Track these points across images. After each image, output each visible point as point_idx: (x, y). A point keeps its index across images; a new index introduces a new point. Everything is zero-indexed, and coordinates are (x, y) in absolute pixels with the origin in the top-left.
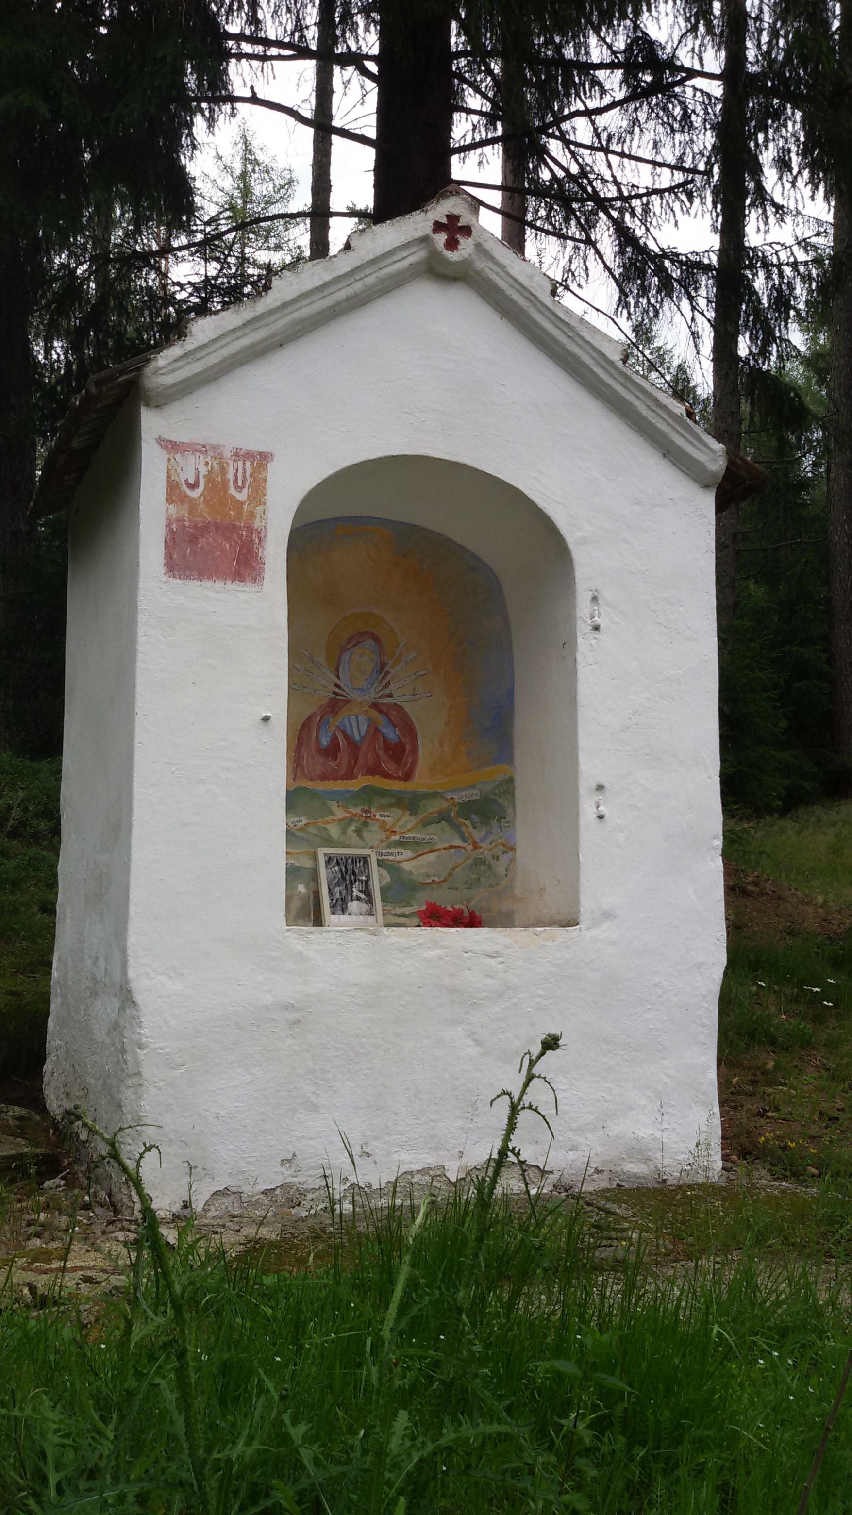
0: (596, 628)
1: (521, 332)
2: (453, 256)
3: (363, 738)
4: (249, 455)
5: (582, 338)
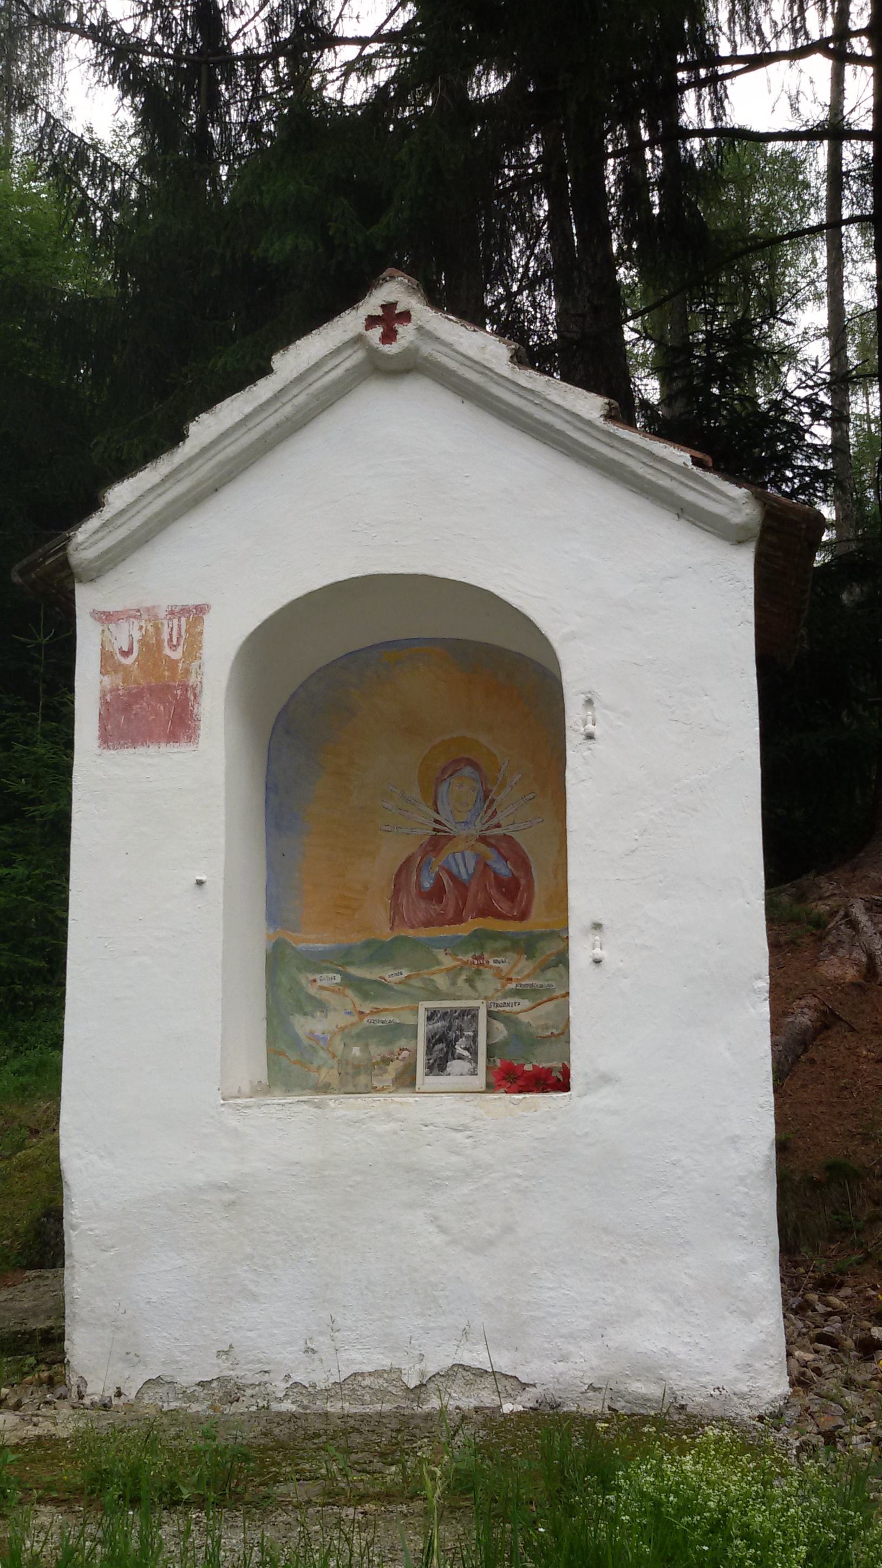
0: (590, 737)
1: (484, 409)
2: (391, 349)
3: (471, 876)
4: (185, 610)
5: (550, 402)
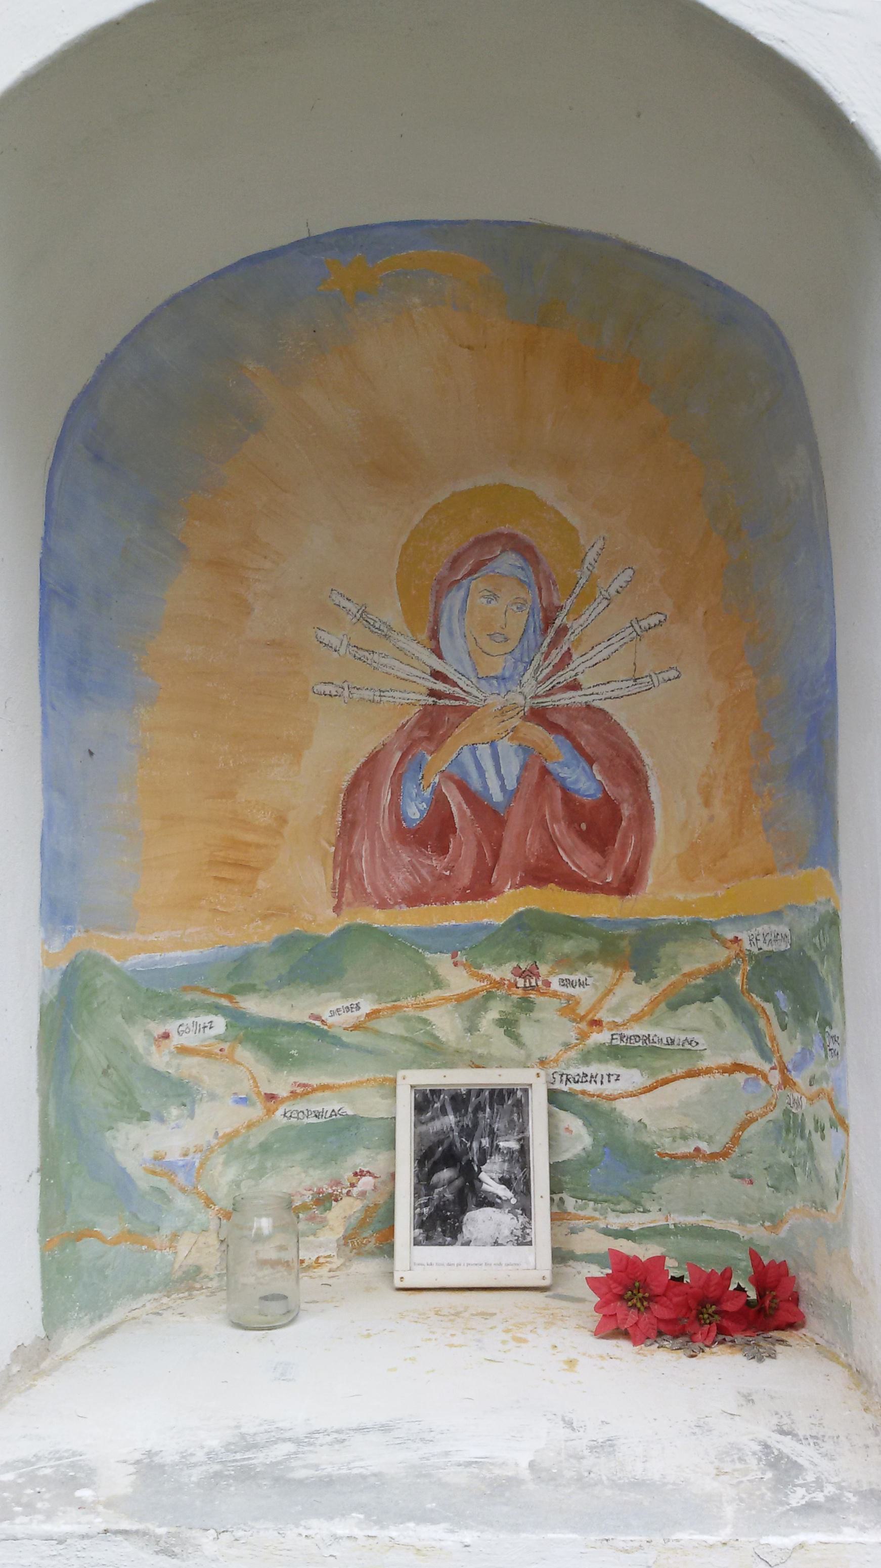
3: (511, 796)
